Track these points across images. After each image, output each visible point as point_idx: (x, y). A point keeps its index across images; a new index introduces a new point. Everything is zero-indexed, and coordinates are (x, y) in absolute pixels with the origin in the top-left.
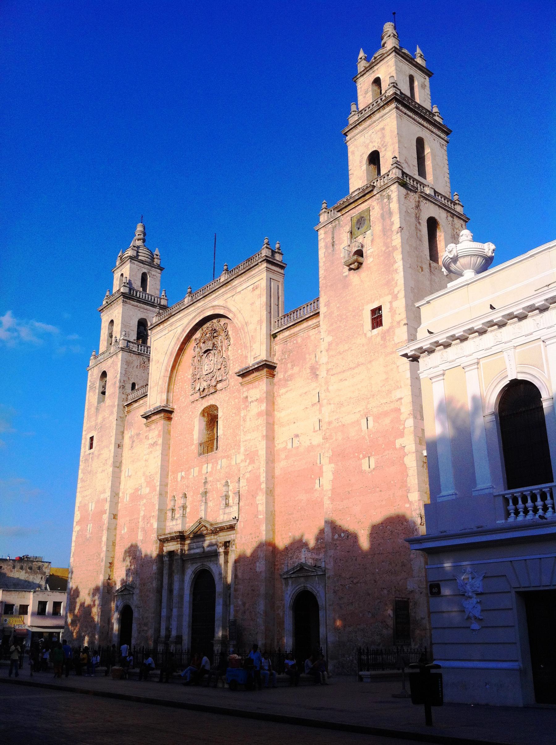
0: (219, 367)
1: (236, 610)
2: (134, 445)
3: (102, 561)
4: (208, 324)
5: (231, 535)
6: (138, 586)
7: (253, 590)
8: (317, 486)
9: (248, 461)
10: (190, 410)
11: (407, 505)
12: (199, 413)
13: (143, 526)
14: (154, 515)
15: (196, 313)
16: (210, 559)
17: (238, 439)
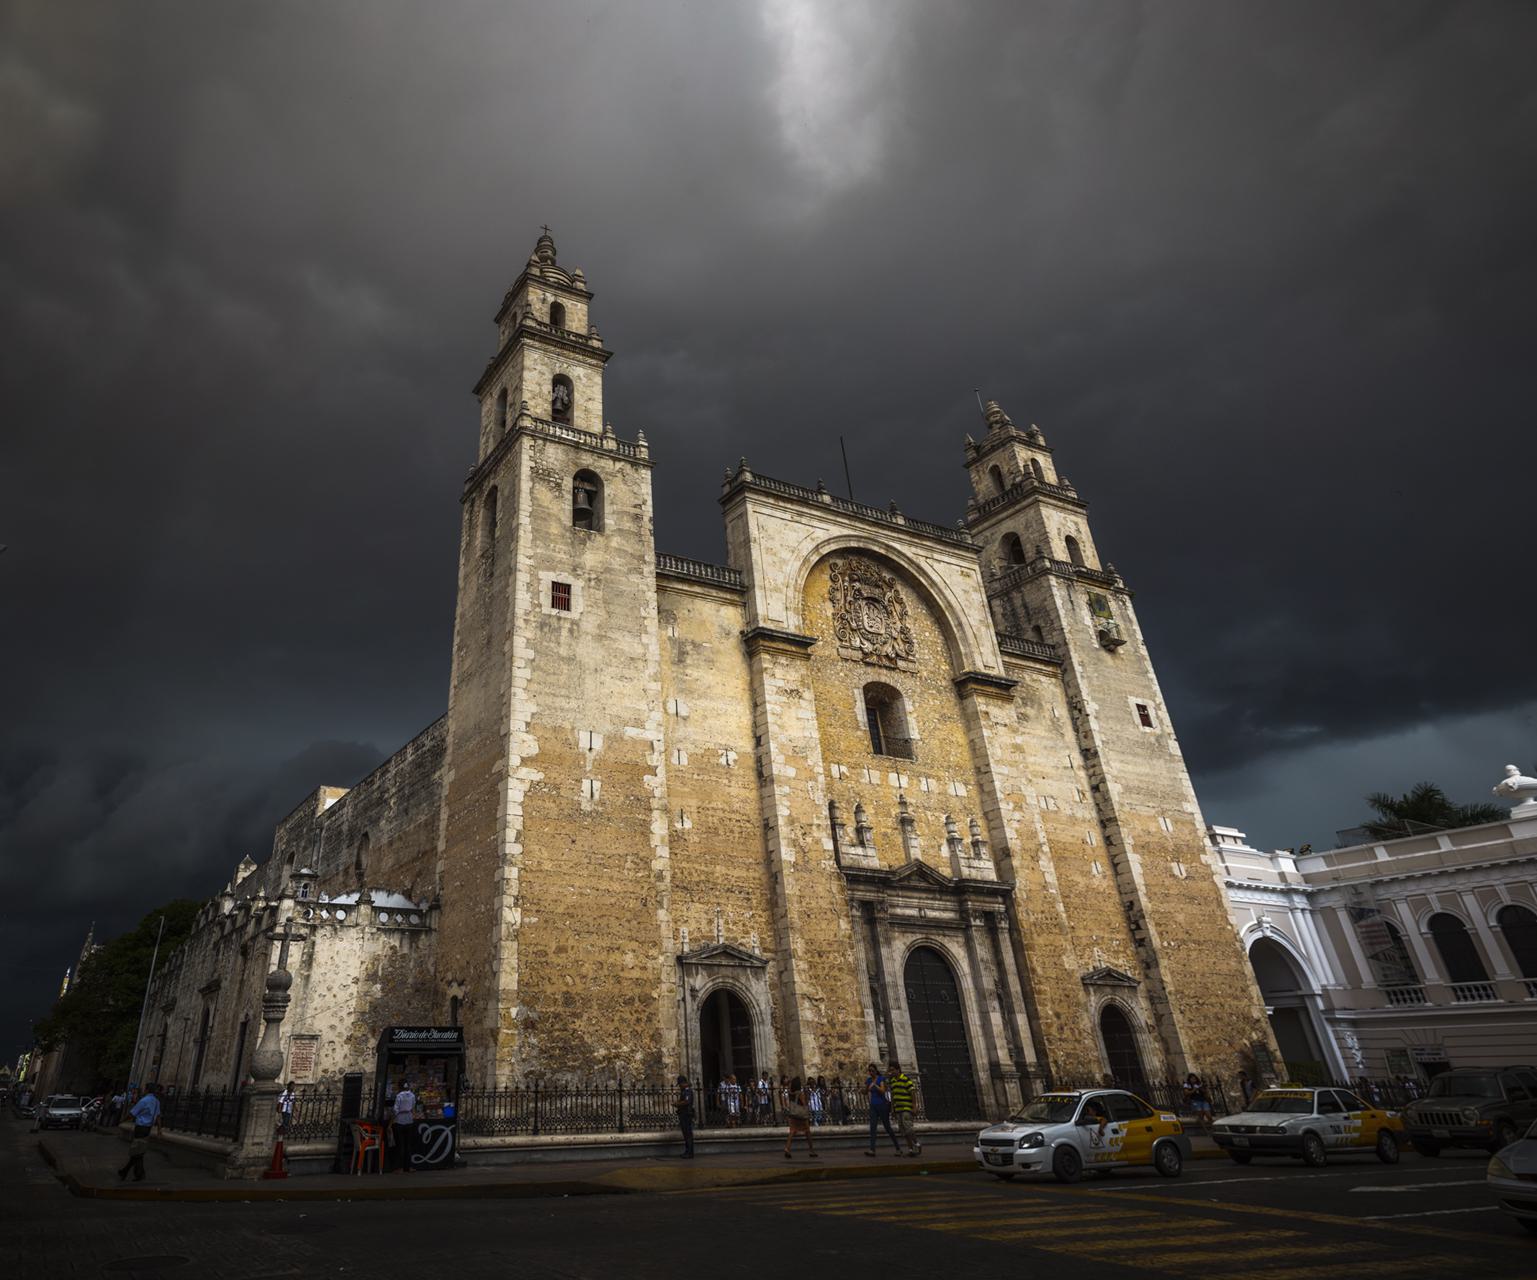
0: (895, 634)
2: (689, 661)
3: (660, 877)
4: (866, 561)
8: (1094, 871)
9: (1011, 806)
10: (839, 668)
11: (1229, 927)
12: (863, 683)
14: (819, 825)
15: (856, 533)
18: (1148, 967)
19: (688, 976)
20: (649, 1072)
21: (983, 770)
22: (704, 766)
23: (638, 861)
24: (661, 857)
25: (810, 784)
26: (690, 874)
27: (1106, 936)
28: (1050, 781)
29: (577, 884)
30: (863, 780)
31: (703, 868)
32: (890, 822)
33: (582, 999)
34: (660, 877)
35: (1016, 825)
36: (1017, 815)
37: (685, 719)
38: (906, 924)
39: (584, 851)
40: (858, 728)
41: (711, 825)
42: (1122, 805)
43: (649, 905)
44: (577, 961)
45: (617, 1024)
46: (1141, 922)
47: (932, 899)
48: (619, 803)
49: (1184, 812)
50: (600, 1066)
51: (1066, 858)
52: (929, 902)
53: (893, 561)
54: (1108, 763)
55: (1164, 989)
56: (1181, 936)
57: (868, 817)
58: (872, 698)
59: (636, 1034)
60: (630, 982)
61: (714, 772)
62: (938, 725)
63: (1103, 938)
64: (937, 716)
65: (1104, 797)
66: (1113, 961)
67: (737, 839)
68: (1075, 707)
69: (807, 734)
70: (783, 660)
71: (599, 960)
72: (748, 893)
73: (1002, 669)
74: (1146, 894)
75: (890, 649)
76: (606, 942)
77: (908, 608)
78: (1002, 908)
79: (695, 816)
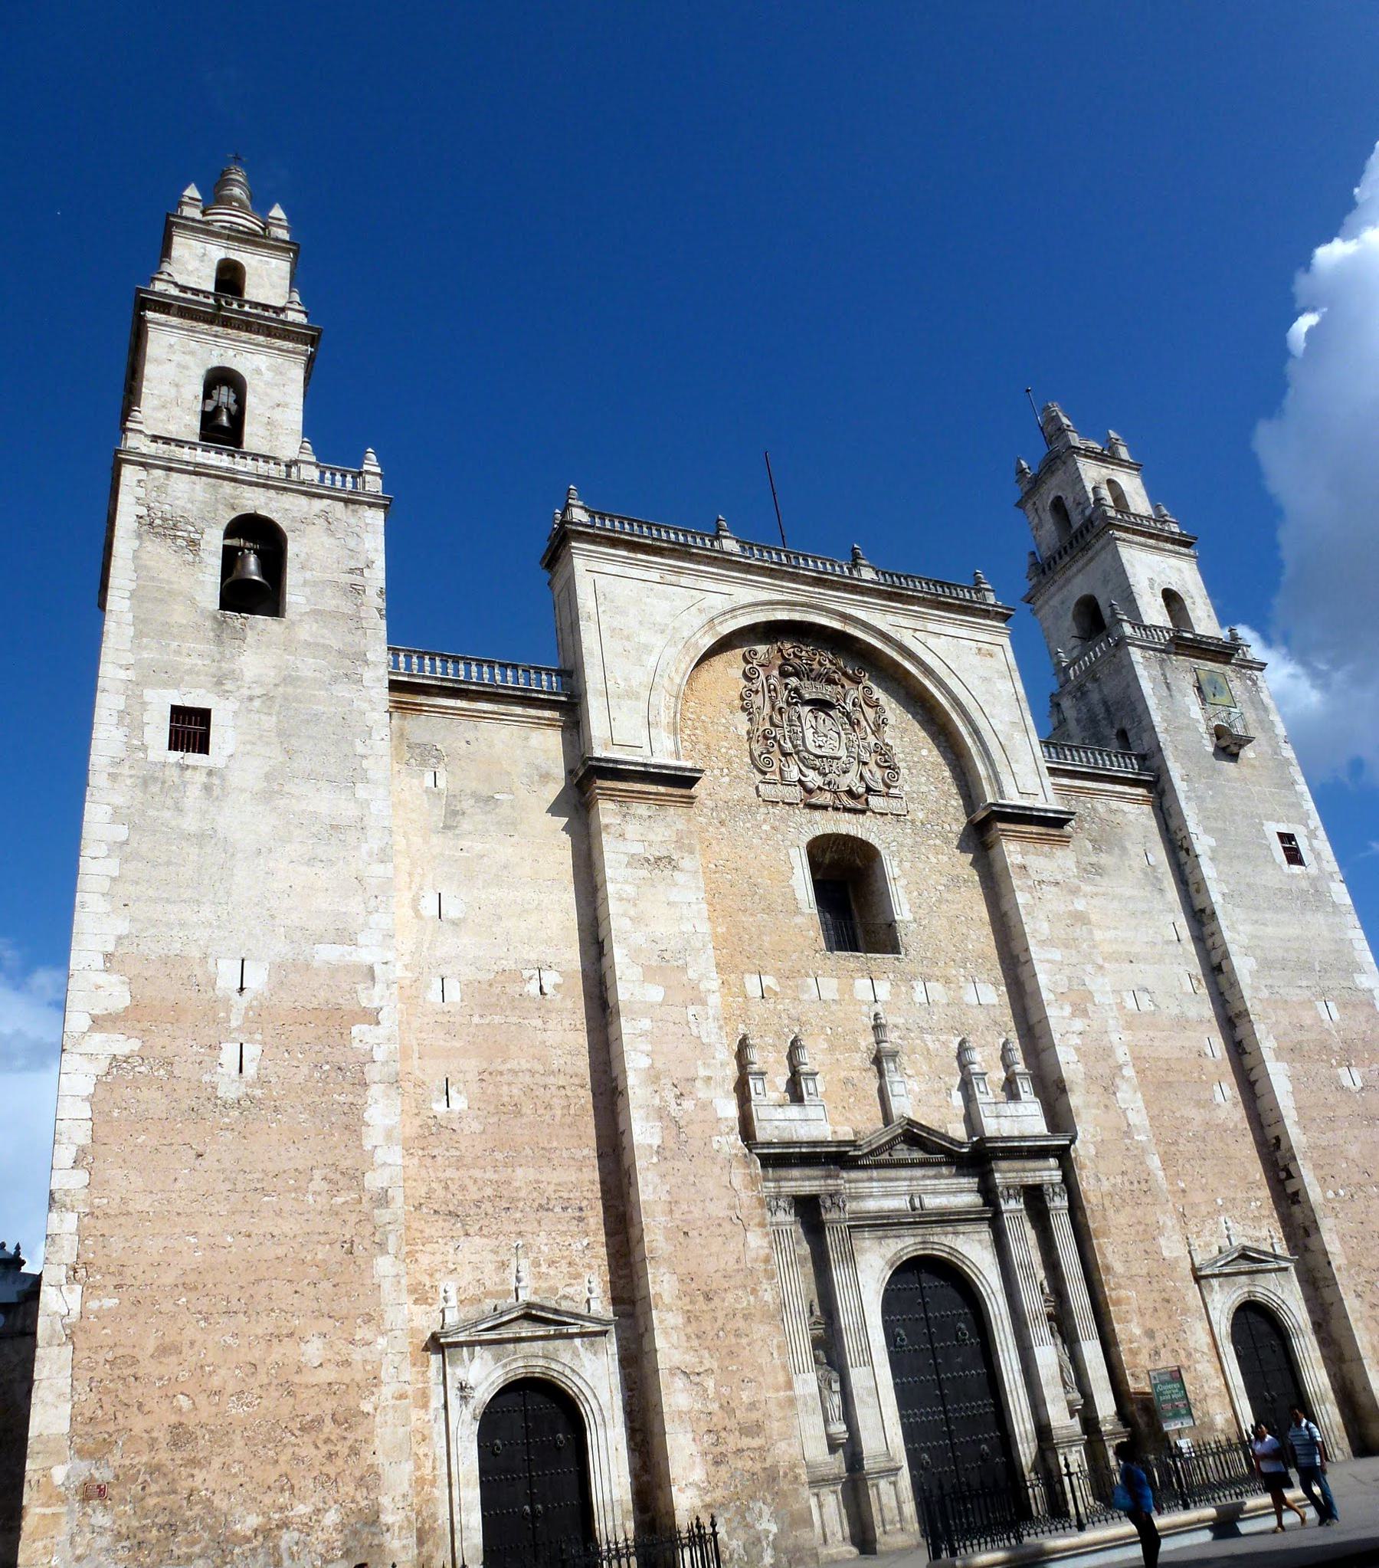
0: (865, 757)
1: (1130, 1349)
2: (466, 825)
5: (1040, 1170)
6: (667, 1299)
7: (1168, 1301)
8: (1219, 1098)
9: (1068, 1010)
12: (810, 837)
13: (657, 1102)
14: (709, 1078)
15: (785, 598)
16: (950, 1229)
17: (970, 947)
18: (1307, 1234)
19: (451, 1365)
20: (351, 1543)
21: (1022, 960)
22: (494, 1000)
23: (338, 1176)
24: (384, 1164)
25: (692, 1010)
26: (463, 1188)
27: (1239, 1195)
28: (1142, 966)
29: (206, 1229)
30: (805, 997)
31: (490, 1175)
32: (861, 1059)
33: (212, 1431)
34: (383, 1199)
35: (1076, 1040)
36: (1078, 1024)
37: (455, 923)
38: (884, 1224)
39: (224, 1171)
40: (797, 911)
41: (506, 1099)
42: (1256, 989)
43: (358, 1250)
44: (202, 1367)
45: (283, 1467)
46: (1292, 1168)
47: (935, 1177)
48: (300, 1078)
49: (1357, 989)
50: (248, 1546)
51: (1170, 1084)
52: (928, 1182)
53: (857, 639)
54: (1232, 927)
55: (1329, 1263)
56: (1357, 1177)
57: (809, 1060)
58: (833, 864)
59: (326, 1481)
60: (312, 1392)
61: (514, 1008)
62: (946, 895)
63: (1234, 1199)
64: (944, 881)
65: (1228, 979)
66: (1251, 1232)
67: (557, 1119)
68: (1178, 847)
69: (687, 927)
70: (641, 809)
71: (249, 1359)
72: (581, 1209)
73: (1050, 794)
74: (1298, 1123)
75: (857, 780)
76: (265, 1325)
77: (888, 714)
78: (1057, 1176)
79: (474, 1087)
